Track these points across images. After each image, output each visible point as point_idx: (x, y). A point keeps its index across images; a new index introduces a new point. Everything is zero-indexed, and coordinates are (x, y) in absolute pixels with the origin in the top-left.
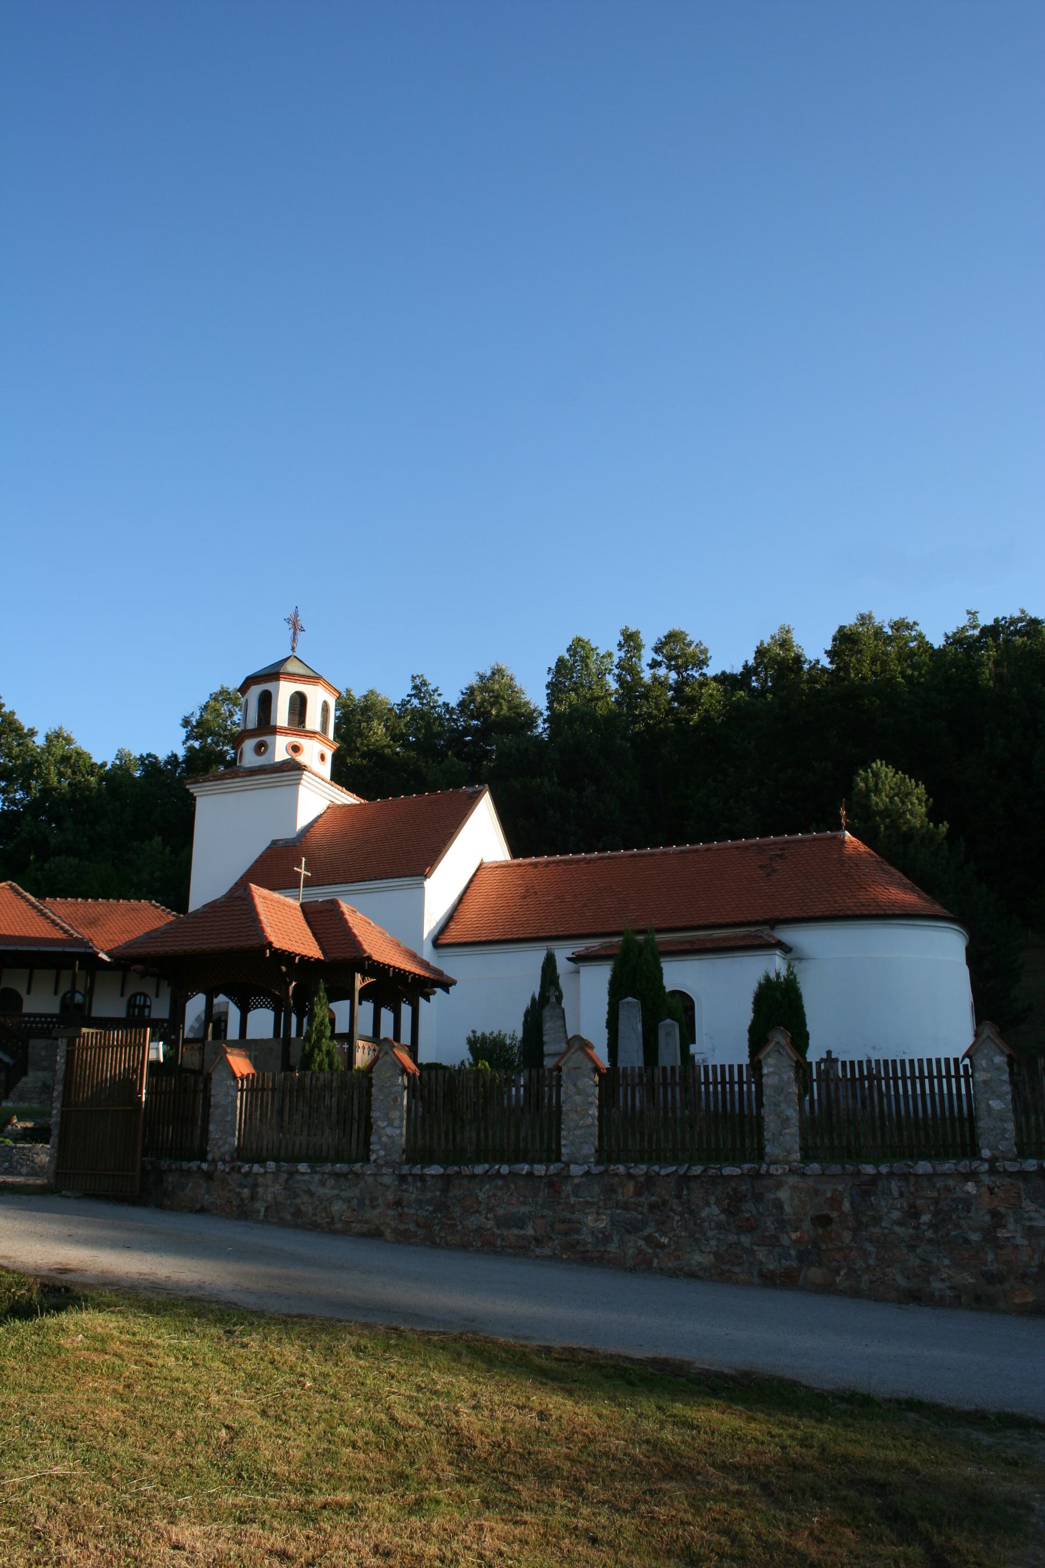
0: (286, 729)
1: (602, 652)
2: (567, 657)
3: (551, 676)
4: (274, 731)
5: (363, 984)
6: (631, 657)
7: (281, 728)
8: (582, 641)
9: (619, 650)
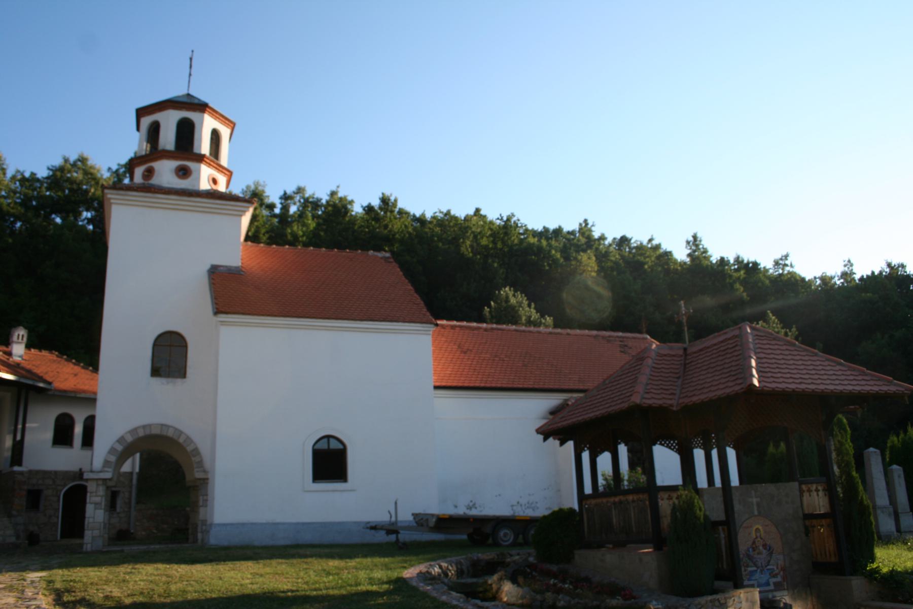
4: (200, 158)
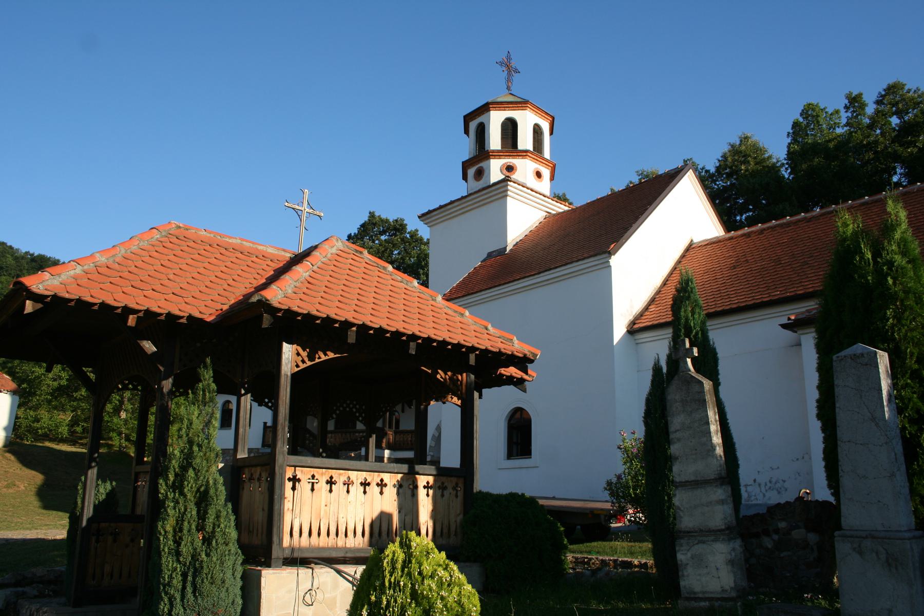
0: (498, 151)
1: (830, 110)
2: (801, 120)
3: (790, 138)
5: (309, 363)
6: (857, 115)
7: (493, 151)
8: (812, 105)
9: (846, 112)
